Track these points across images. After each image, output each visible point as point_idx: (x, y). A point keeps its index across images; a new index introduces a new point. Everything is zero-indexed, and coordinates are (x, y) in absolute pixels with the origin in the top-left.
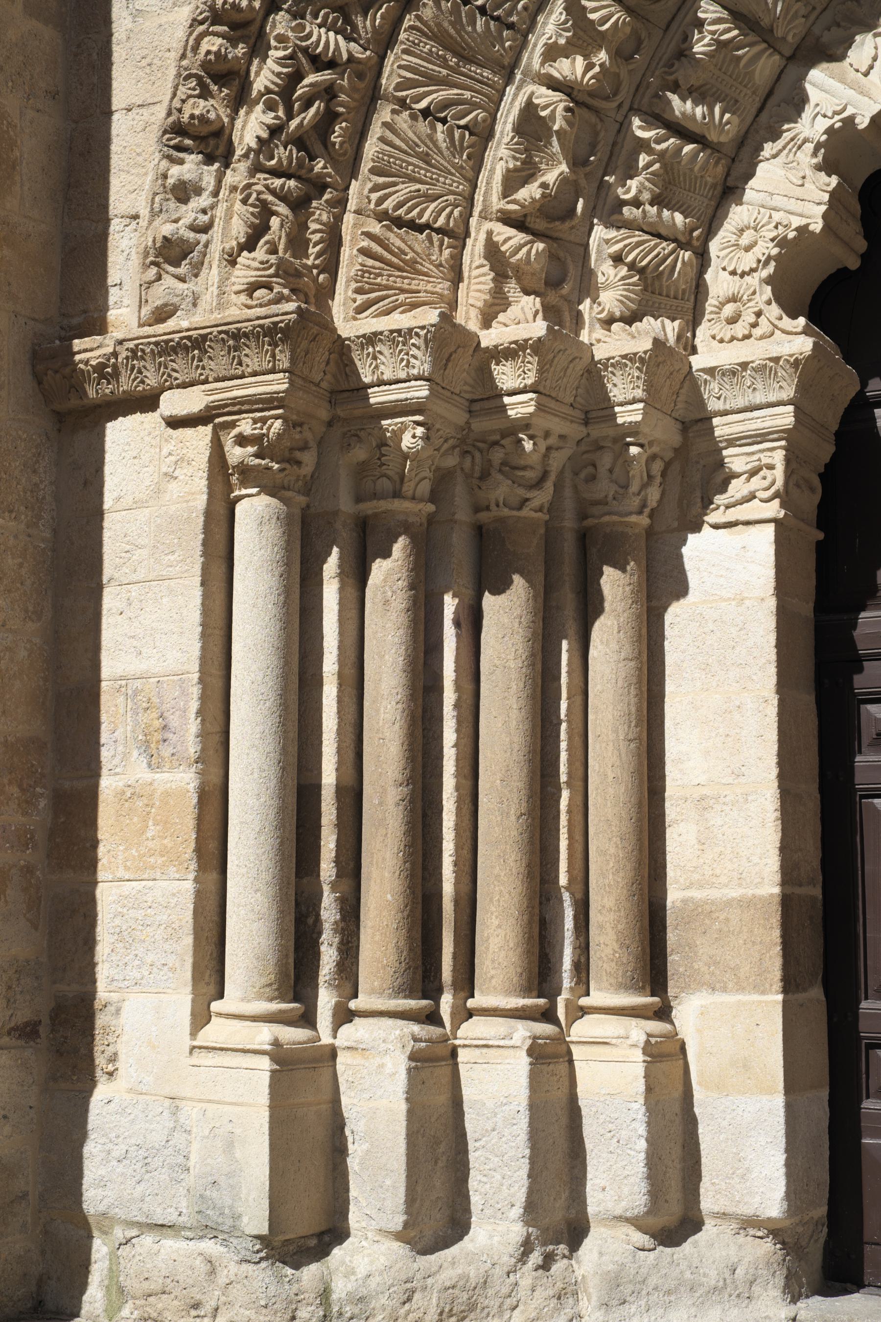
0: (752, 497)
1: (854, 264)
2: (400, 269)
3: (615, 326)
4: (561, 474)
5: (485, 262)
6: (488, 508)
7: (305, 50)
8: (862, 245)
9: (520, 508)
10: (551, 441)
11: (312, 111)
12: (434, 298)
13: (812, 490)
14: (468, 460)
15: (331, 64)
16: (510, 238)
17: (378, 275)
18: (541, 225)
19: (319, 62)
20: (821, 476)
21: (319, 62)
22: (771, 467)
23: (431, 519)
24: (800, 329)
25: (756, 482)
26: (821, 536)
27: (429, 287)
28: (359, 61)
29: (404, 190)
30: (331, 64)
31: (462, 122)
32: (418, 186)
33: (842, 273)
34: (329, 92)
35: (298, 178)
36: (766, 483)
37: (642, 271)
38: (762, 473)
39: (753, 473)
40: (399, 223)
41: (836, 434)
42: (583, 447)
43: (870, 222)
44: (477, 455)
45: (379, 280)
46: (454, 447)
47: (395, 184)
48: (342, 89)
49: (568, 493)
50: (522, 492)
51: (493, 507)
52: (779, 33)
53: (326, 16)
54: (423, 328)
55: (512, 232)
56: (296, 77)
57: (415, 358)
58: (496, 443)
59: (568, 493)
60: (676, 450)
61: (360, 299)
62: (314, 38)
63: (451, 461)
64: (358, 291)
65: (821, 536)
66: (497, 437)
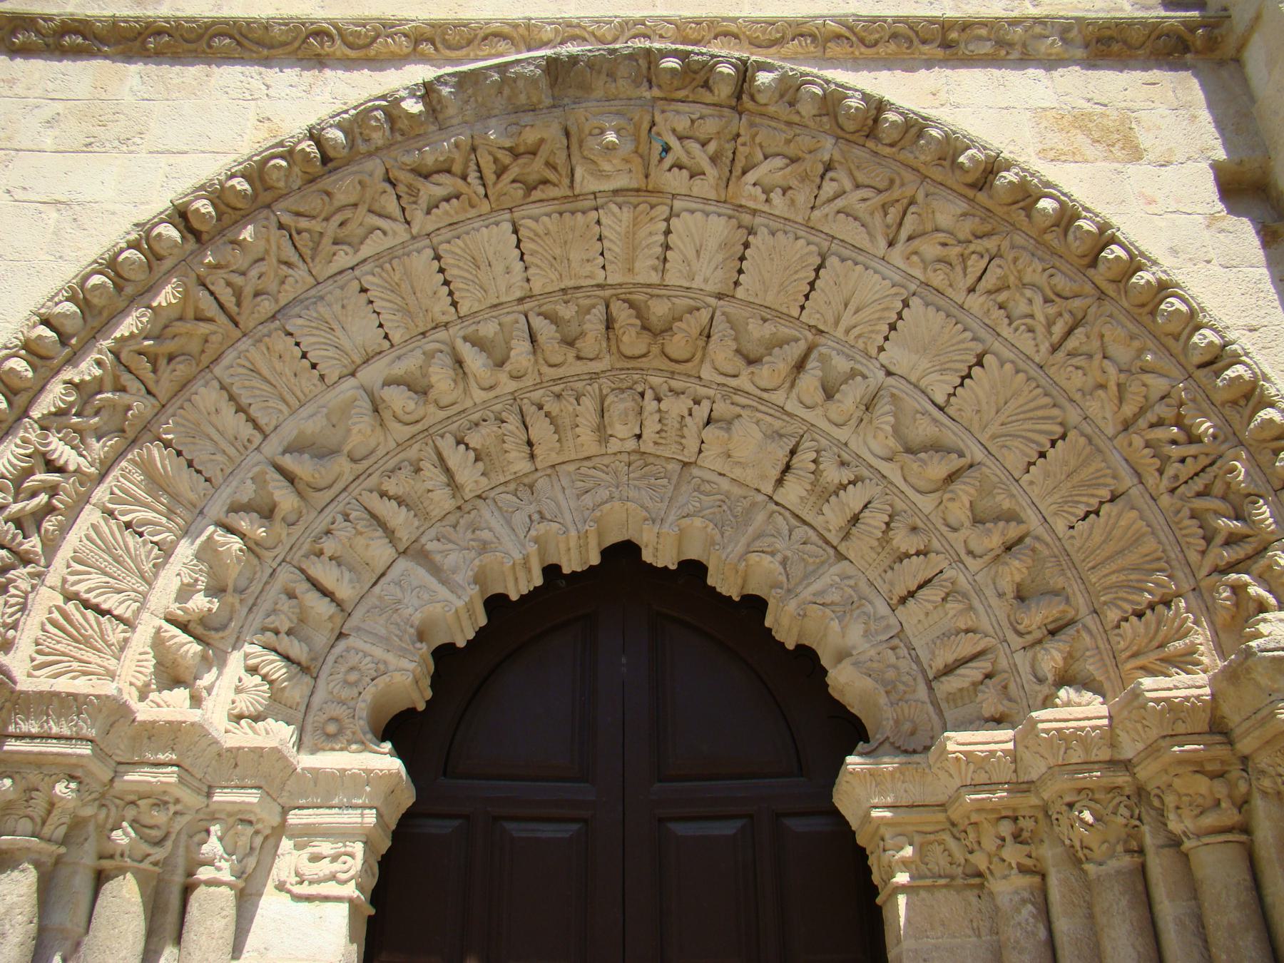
0: (333, 877)
1: (421, 707)
2: (77, 641)
3: (243, 722)
4: (179, 833)
5: (149, 650)
6: (112, 857)
7: (44, 454)
8: (429, 694)
9: (141, 861)
10: (179, 807)
11: (36, 501)
12: (101, 671)
13: (373, 875)
14: (104, 811)
15: (61, 470)
16: (174, 637)
17: (58, 642)
18: (199, 630)
19: (51, 466)
20: (379, 863)
21: (51, 466)
22: (352, 856)
23: (58, 861)
24: (386, 750)
25: (337, 866)
26: (372, 911)
27: (99, 661)
28: (84, 474)
29: (96, 579)
30: (61, 470)
31: (155, 539)
32: (107, 579)
33: (411, 711)
34: (53, 490)
35: (10, 550)
36: (345, 867)
37: (271, 683)
38: (344, 858)
39: (335, 859)
40: (87, 605)
41: (394, 832)
42: (201, 816)
43: (437, 681)
44: (113, 809)
45: (58, 647)
46: (95, 800)
47: (89, 573)
48: (65, 490)
49: (181, 851)
50: (146, 848)
51: (117, 857)
52: (398, 534)
53: (67, 435)
54: (98, 697)
55: (178, 632)
56: (29, 473)
57: (85, 722)
58: (133, 803)
59: (181, 851)
60: (273, 828)
61: (41, 659)
62: (52, 447)
63: (88, 812)
64: (39, 652)
65: (372, 911)
66: (132, 797)
